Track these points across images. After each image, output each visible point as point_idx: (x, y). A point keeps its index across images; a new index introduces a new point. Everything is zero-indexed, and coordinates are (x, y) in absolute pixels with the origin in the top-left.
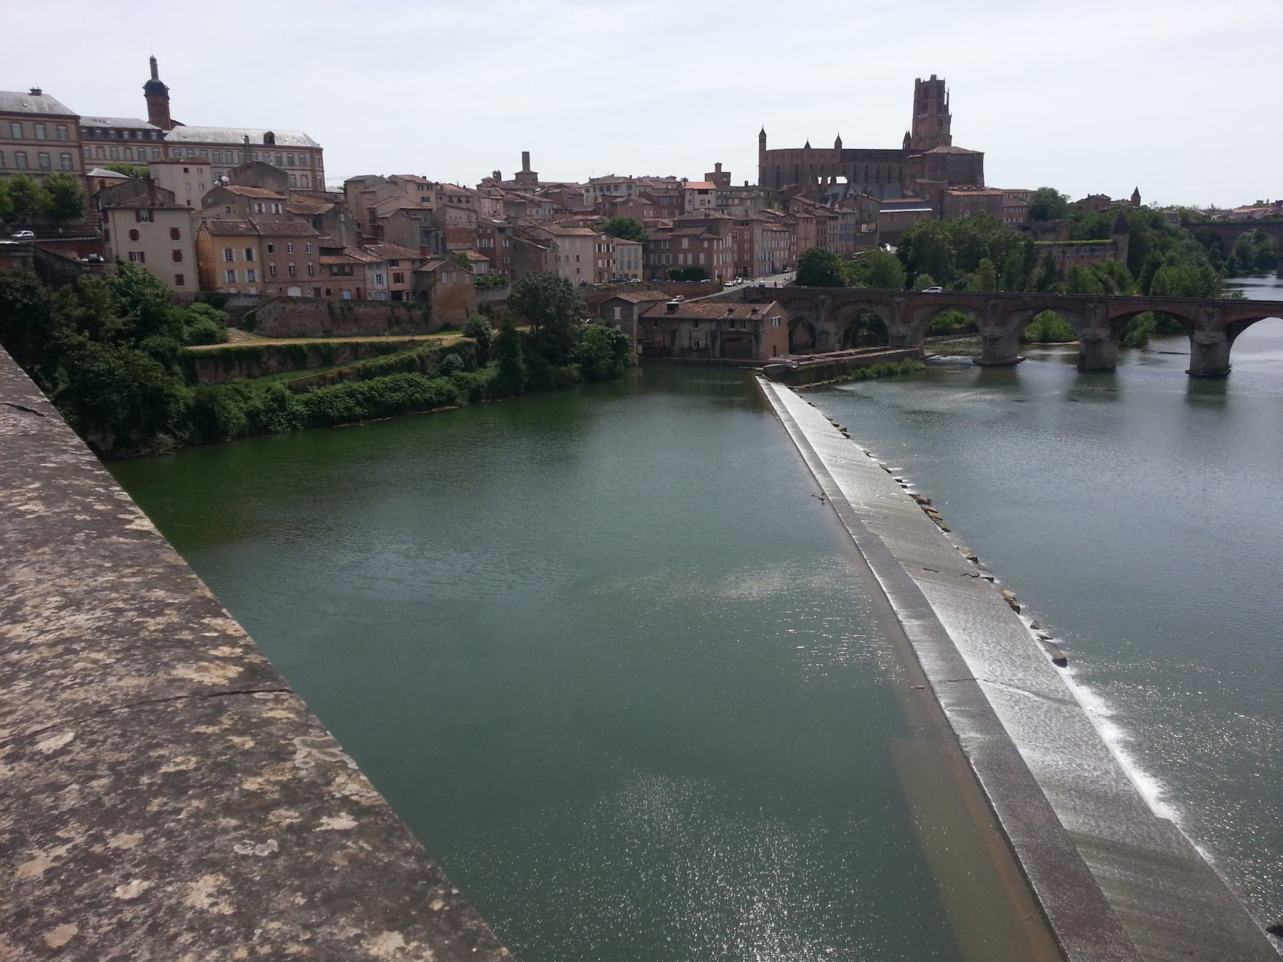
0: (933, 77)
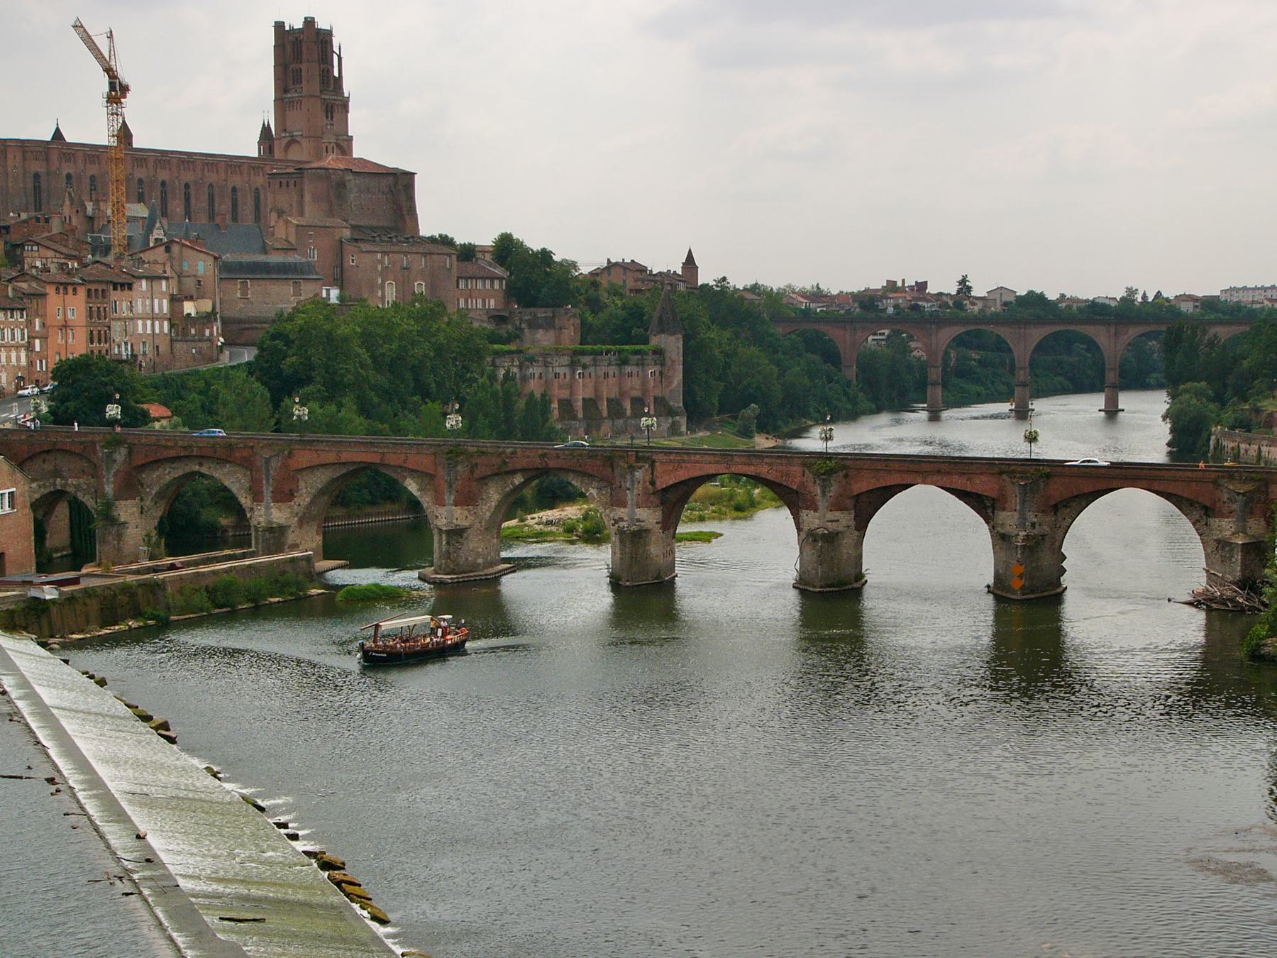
0: (309, 22)
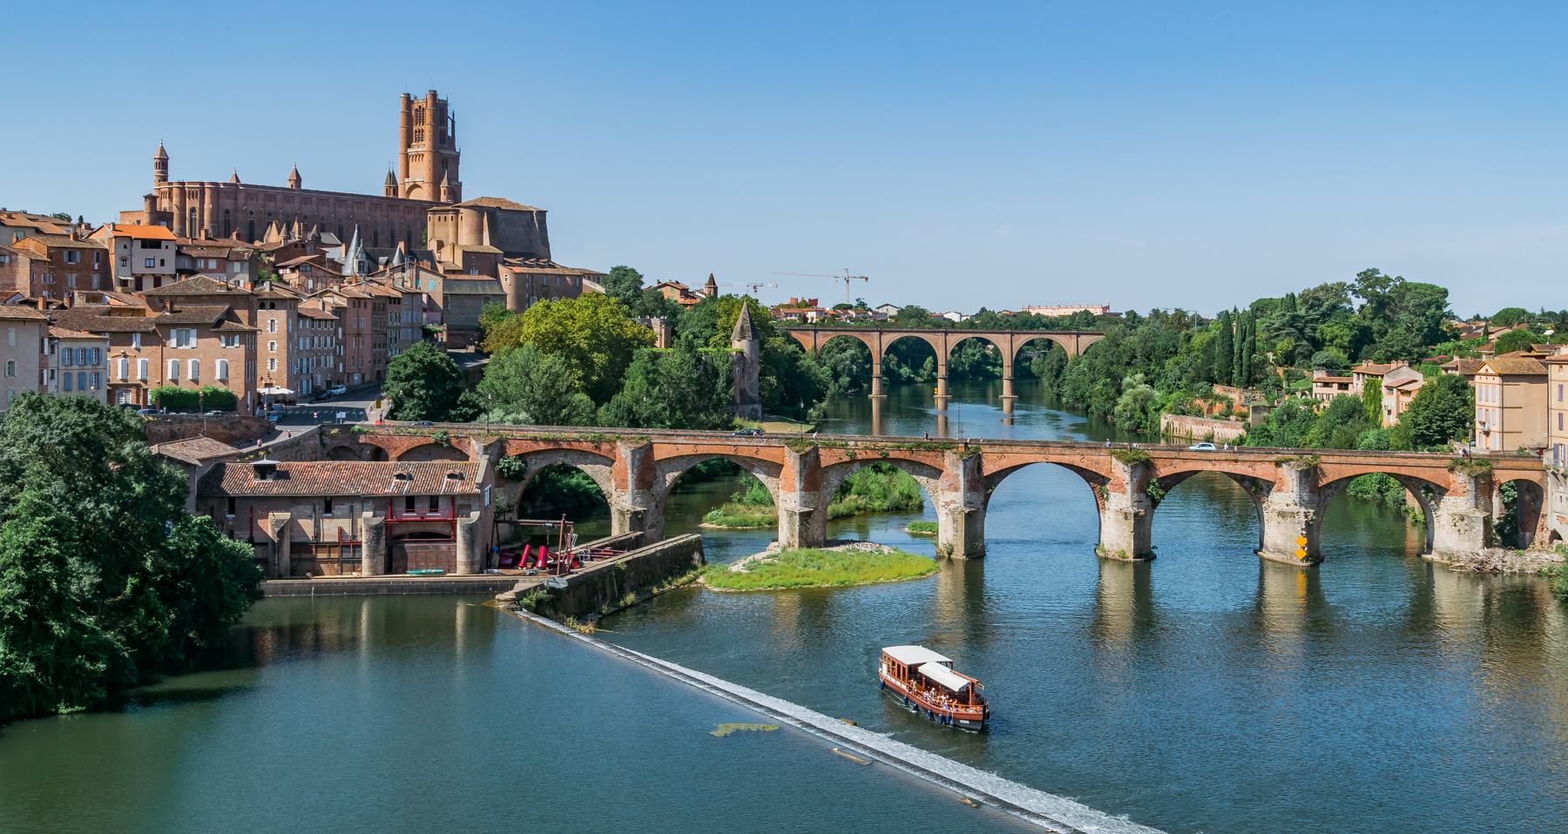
0: (434, 94)
